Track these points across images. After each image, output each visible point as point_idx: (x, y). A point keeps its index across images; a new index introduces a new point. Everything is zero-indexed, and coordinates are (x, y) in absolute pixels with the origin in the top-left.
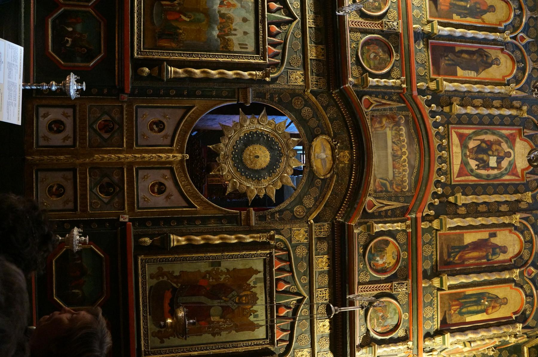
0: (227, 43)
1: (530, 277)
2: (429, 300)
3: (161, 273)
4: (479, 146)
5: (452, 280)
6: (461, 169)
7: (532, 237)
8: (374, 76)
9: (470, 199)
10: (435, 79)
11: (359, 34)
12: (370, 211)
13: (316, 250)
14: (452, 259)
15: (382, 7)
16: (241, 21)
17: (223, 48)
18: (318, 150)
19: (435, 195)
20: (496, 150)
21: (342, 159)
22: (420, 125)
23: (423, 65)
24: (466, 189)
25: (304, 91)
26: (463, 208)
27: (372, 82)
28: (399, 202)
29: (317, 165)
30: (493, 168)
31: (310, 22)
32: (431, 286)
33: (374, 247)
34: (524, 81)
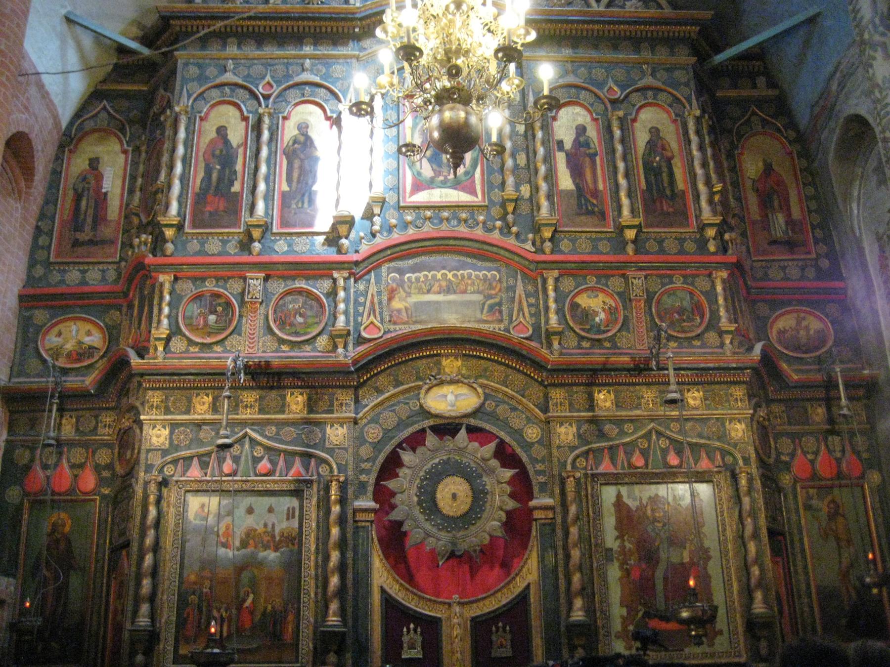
3: (622, 635)
4: (429, 160)
6: (464, 189)
16: (252, 516)
17: (293, 544)
21: (455, 370)
26: (522, 188)
28: (516, 286)
32: (634, 242)
33: (581, 324)
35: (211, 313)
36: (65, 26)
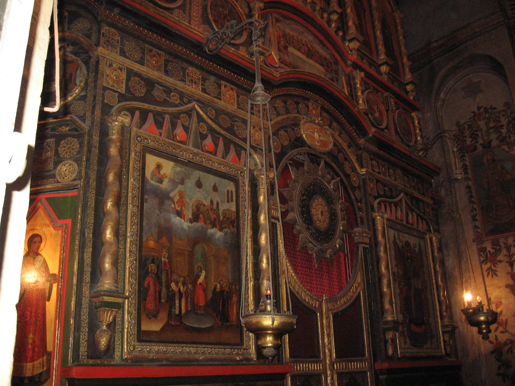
0: (228, 219)
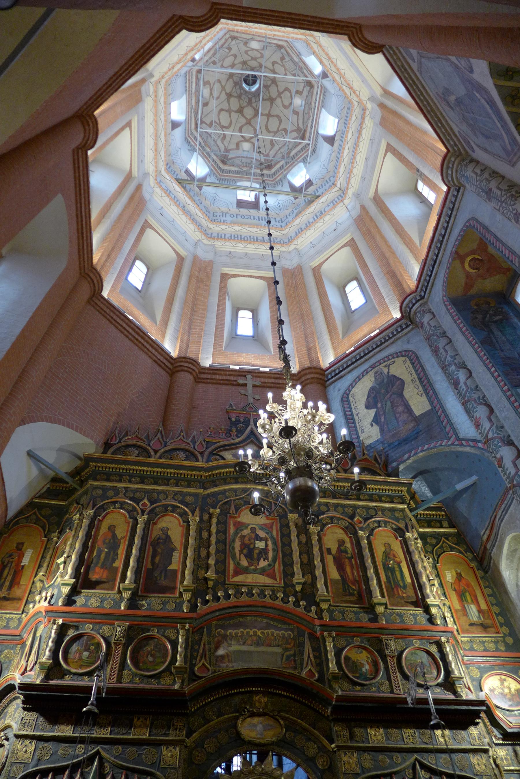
1: (363, 521)
2: (398, 617)
4: (246, 556)
5: (376, 593)
6: (268, 576)
7: (328, 517)
8: (174, 659)
9: (297, 569)
10: (180, 592)
11: (125, 672)
12: (317, 675)
13: (363, 742)
14: (356, 592)
15: (96, 641)
18: (253, 734)
19: (296, 604)
20: (249, 540)
22: (226, 614)
23: (164, 604)
24: (288, 574)
25: (186, 747)
27: (181, 661)
29: (270, 736)
30: (267, 545)
31: (105, 733)
34: (185, 508)
35: (86, 650)
36: (25, 457)
